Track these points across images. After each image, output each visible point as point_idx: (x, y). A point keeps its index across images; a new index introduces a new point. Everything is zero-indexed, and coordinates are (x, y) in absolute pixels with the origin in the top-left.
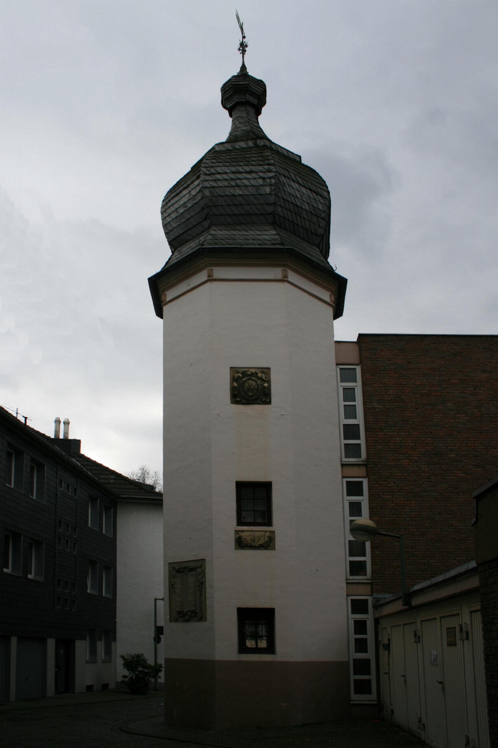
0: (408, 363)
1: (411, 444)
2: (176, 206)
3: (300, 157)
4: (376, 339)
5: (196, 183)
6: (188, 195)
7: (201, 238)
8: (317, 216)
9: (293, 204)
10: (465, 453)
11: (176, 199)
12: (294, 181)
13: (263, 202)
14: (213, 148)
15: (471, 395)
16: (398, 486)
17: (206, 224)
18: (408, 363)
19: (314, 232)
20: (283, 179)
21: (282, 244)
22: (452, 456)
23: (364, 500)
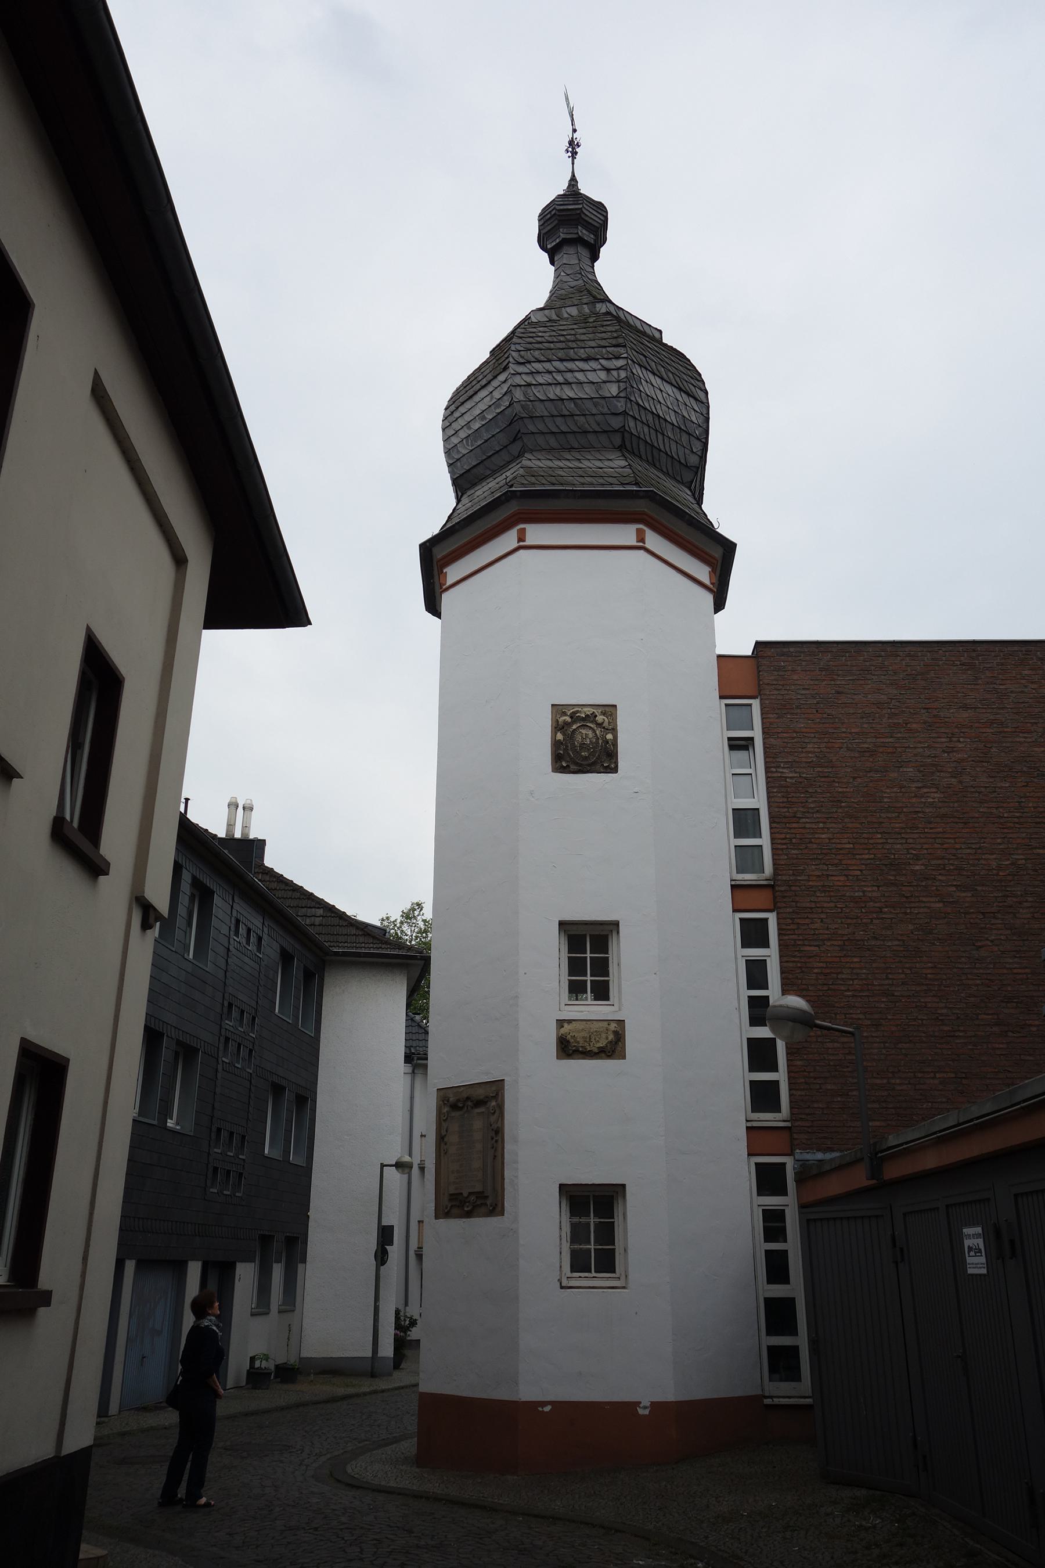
0: (838, 693)
1: (848, 846)
2: (468, 417)
3: (660, 332)
4: (785, 650)
5: (502, 377)
6: (488, 398)
7: (508, 474)
8: (689, 434)
9: (652, 413)
10: (940, 862)
11: (468, 405)
12: (654, 374)
13: (606, 410)
14: (527, 318)
15: (944, 751)
16: (828, 929)
17: (515, 449)
18: (838, 693)
19: (683, 461)
20: (637, 370)
21: (637, 484)
22: (917, 868)
23: (771, 955)
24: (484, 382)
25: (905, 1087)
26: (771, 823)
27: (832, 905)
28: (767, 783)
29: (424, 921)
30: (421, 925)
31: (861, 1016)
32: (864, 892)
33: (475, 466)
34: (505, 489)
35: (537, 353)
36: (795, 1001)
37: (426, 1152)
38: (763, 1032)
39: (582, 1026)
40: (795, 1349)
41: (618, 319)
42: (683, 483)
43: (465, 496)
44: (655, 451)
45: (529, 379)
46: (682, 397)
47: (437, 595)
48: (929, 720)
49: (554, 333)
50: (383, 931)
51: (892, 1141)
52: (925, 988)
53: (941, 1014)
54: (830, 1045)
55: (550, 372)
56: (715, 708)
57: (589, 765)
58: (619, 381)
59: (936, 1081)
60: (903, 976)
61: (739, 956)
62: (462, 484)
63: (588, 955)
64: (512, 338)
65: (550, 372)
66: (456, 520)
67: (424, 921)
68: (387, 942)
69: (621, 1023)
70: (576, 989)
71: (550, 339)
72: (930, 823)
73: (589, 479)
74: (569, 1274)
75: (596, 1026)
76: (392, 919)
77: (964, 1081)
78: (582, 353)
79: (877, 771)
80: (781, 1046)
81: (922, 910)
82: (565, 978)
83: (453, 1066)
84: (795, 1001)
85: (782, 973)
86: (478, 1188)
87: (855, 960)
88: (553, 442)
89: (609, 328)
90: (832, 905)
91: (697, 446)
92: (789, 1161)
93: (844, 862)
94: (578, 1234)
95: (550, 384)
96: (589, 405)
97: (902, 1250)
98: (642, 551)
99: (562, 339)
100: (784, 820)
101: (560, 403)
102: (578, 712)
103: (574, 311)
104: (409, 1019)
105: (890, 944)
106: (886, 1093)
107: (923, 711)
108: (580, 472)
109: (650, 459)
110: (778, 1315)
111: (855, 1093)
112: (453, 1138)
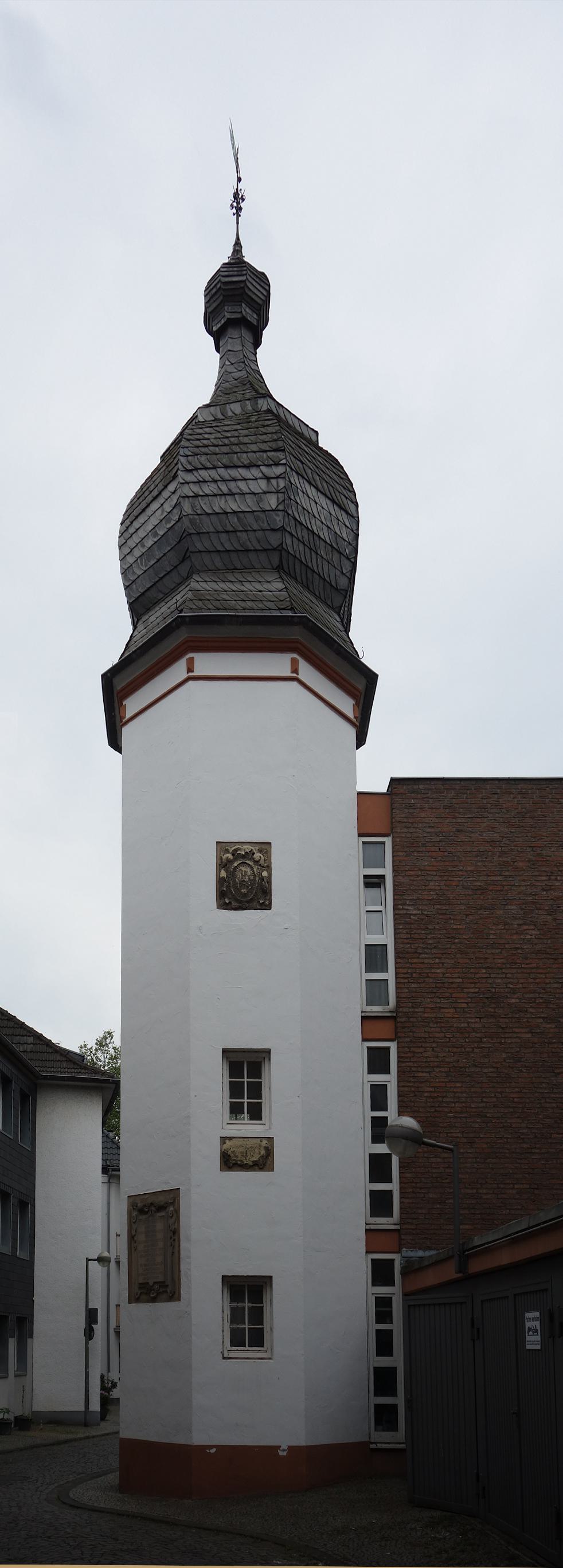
0: (458, 831)
1: (458, 980)
2: (141, 533)
3: (317, 433)
4: (415, 787)
5: (171, 487)
6: (159, 511)
7: (178, 597)
8: (340, 553)
9: (308, 528)
10: (531, 995)
11: (141, 519)
12: (310, 483)
13: (265, 526)
14: (194, 417)
15: (543, 890)
16: (437, 1057)
17: (184, 569)
18: (458, 831)
19: (333, 584)
20: (295, 479)
21: (292, 609)
22: (513, 1001)
23: (391, 1080)
24: (155, 493)
25: (489, 1196)
26: (396, 958)
27: (442, 1035)
28: (395, 919)
29: (114, 1048)
30: (112, 1052)
31: (459, 1135)
32: (468, 1023)
33: (148, 589)
34: (176, 615)
35: (203, 458)
36: (409, 1122)
37: (120, 1249)
38: (382, 1149)
39: (240, 1142)
40: (395, 1407)
41: (277, 417)
42: (333, 608)
43: (140, 622)
44: (309, 572)
45: (196, 489)
46: (335, 511)
47: (118, 728)
48: (534, 859)
49: (219, 435)
50: (82, 1057)
51: (477, 1241)
52: (511, 1110)
53: (523, 1134)
54: (434, 1160)
55: (215, 481)
56: (354, 844)
57: (248, 902)
58: (277, 492)
59: (514, 1192)
60: (495, 1099)
61: (365, 1082)
62: (138, 608)
63: (246, 1080)
64: (180, 441)
65: (215, 481)
66: (133, 649)
67: (114, 1048)
68: (85, 1068)
69: (271, 1139)
70: (236, 1110)
71: (215, 442)
72: (527, 958)
73: (250, 604)
74: (229, 1348)
75: (251, 1142)
76: (89, 1047)
77: (536, 1192)
78: (245, 459)
79: (486, 909)
80: (395, 1160)
81: (514, 1040)
82: (227, 1100)
83: (140, 1177)
84: (409, 1122)
85: (399, 1096)
86: (161, 1279)
87: (458, 1085)
88: (217, 561)
89: (270, 429)
90: (442, 1035)
91: (347, 567)
92: (397, 1258)
93: (454, 995)
94: (236, 1316)
95: (215, 495)
96: (250, 519)
97: (478, 1330)
98: (295, 683)
99: (226, 441)
100: (407, 956)
101: (224, 517)
102: (238, 849)
103: (236, 408)
104: (105, 1136)
105: (486, 1070)
106: (474, 1201)
107: (529, 850)
108: (243, 597)
109: (304, 580)
110: (384, 1380)
111: (451, 1201)
112: (141, 1238)
